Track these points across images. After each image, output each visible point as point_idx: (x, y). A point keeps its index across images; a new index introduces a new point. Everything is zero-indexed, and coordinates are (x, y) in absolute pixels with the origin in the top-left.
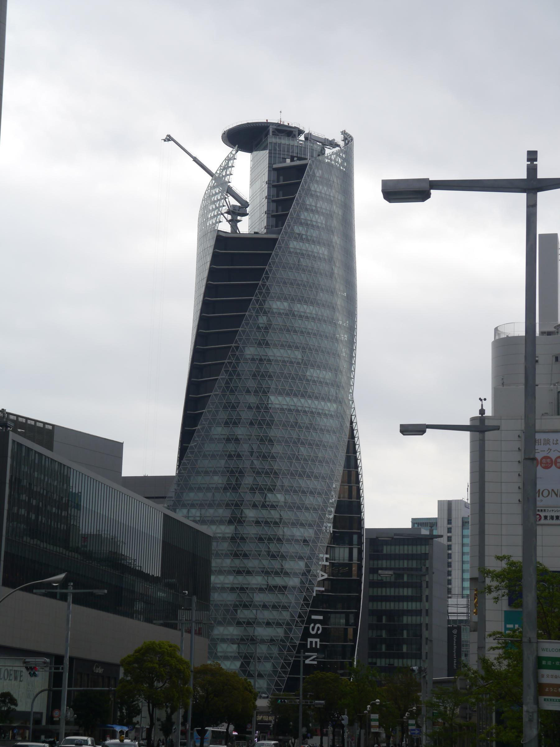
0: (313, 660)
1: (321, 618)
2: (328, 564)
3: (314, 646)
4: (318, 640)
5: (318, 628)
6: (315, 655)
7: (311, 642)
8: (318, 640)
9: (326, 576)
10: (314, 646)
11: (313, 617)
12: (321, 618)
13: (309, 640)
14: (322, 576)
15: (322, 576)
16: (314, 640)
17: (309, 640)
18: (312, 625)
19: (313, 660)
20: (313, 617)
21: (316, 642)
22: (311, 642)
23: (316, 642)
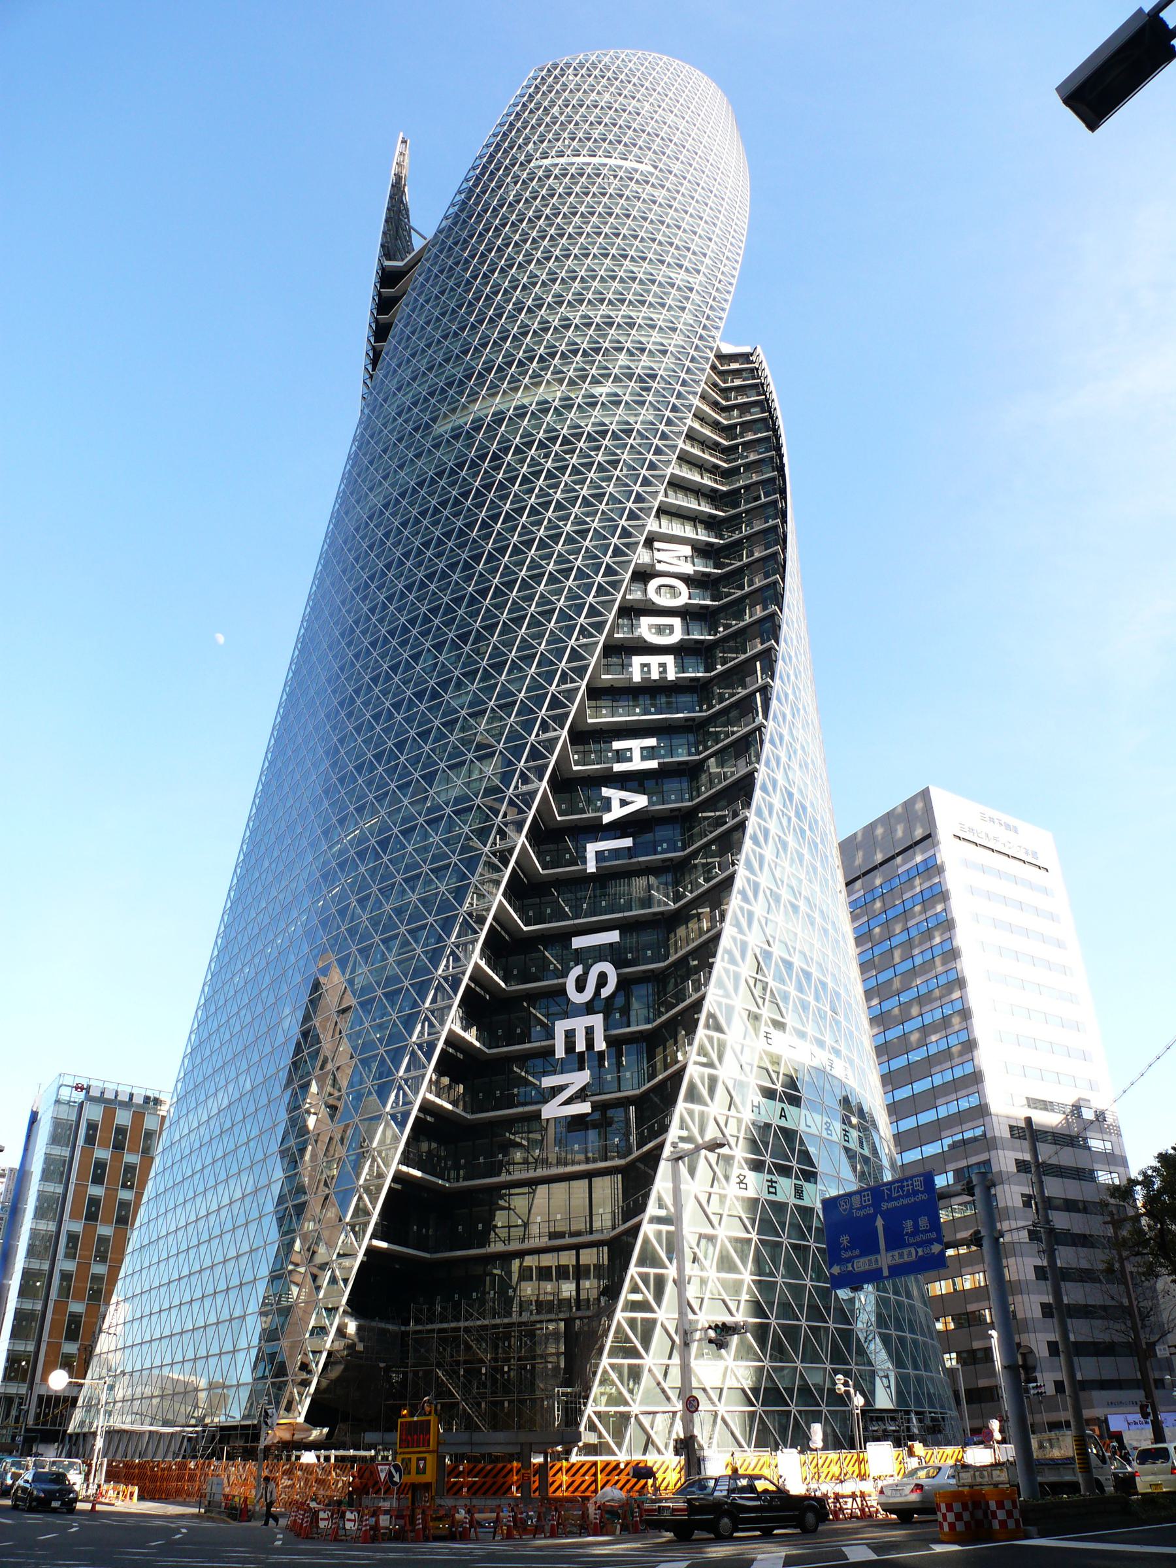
0: (556, 1091)
1: (613, 936)
2: (653, 764)
3: (581, 1046)
4: (597, 1021)
5: (602, 979)
6: (580, 1079)
7: (570, 1035)
8: (597, 1021)
9: (640, 801)
10: (581, 1046)
11: (578, 942)
12: (613, 936)
13: (561, 1027)
14: (624, 803)
15: (624, 803)
16: (579, 1024)
17: (561, 1027)
18: (578, 970)
19: (556, 1091)
20: (578, 942)
21: (590, 1031)
22: (570, 1035)
23: (590, 1031)
